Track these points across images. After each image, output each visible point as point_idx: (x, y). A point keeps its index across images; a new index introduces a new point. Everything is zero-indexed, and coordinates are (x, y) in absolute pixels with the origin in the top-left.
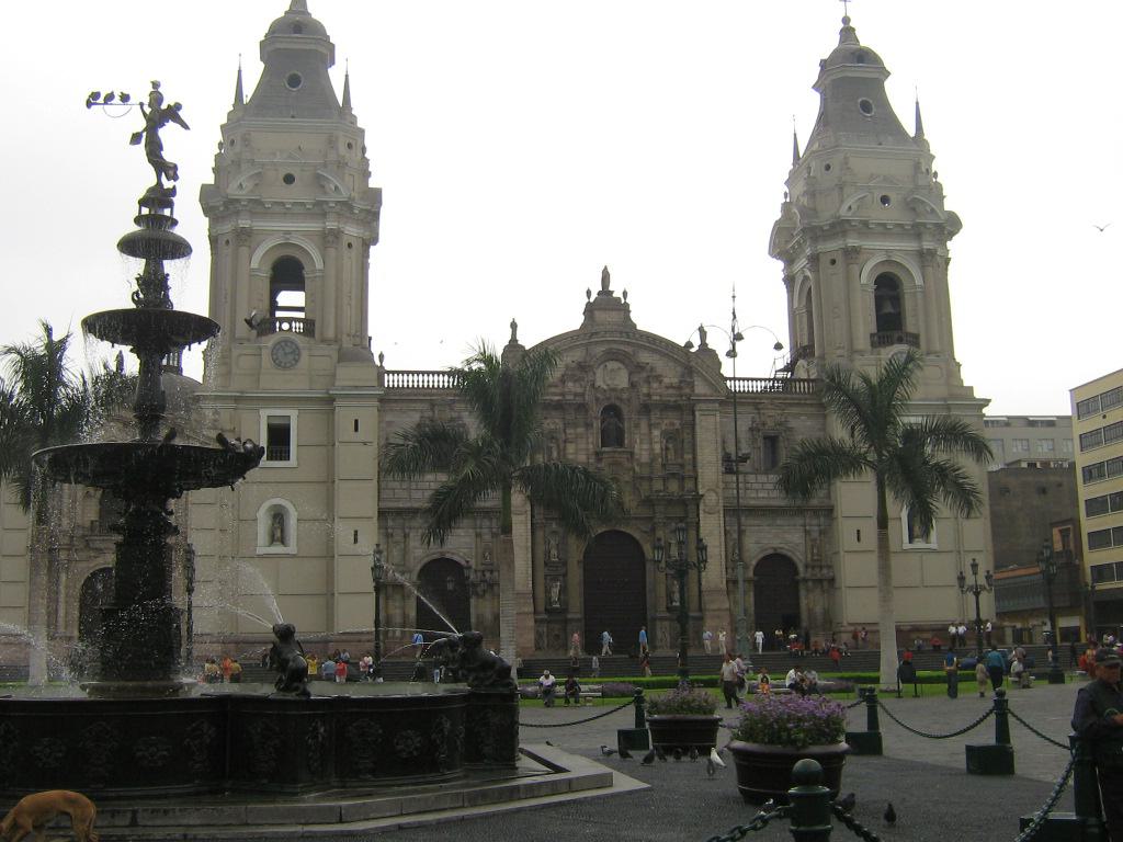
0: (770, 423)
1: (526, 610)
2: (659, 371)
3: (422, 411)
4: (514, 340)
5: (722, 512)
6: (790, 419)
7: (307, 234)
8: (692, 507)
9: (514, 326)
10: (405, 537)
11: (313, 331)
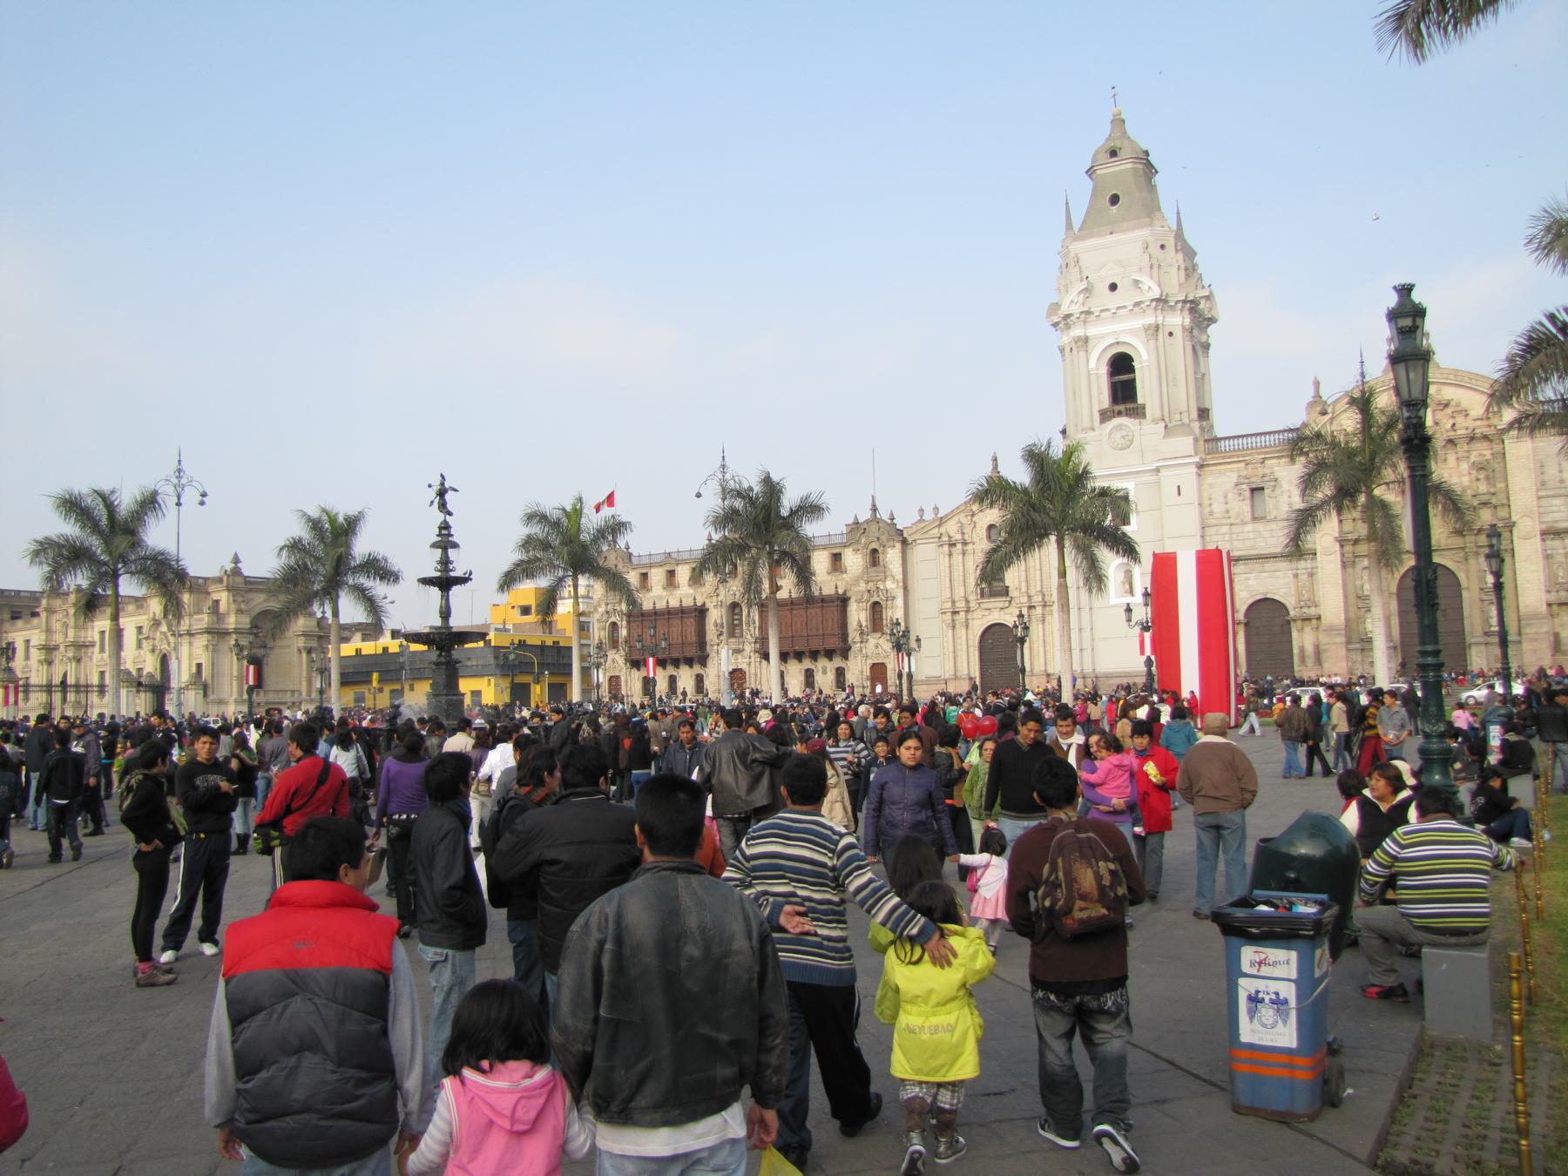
2: (1464, 405)
4: (1317, 396)
7: (1131, 332)
8: (1505, 535)
9: (1317, 384)
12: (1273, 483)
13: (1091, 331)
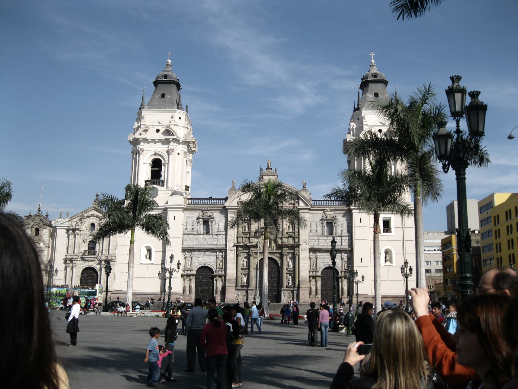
0: (329, 217)
1: (231, 285)
5: (308, 250)
6: (337, 215)
10: (191, 258)
12: (213, 219)
13: (145, 148)
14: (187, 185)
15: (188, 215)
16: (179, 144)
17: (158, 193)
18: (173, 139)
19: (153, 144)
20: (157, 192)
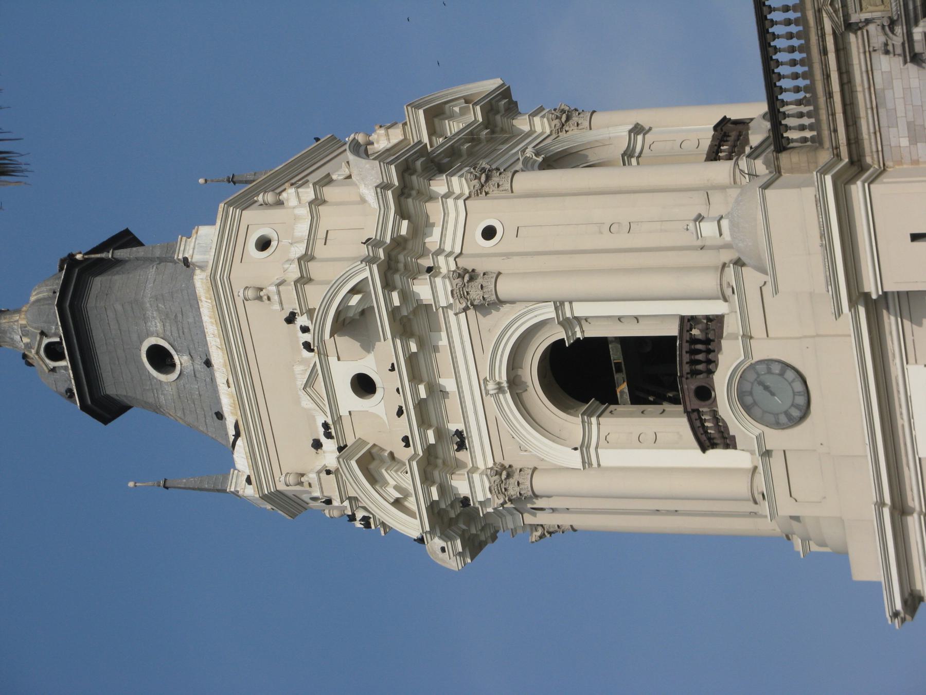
3: (869, 52)
11: (709, 319)
14: (707, 138)
15: (898, 138)
16: (420, 228)
17: (768, 362)
18: (388, 286)
19: (452, 405)
20: (762, 368)
